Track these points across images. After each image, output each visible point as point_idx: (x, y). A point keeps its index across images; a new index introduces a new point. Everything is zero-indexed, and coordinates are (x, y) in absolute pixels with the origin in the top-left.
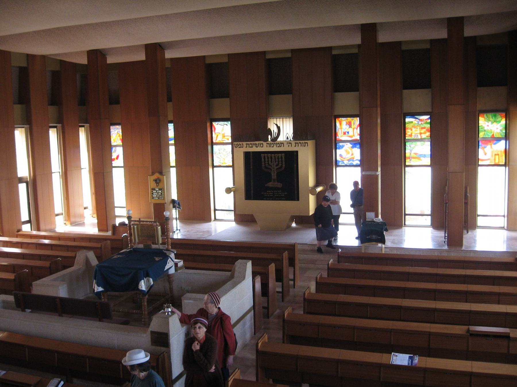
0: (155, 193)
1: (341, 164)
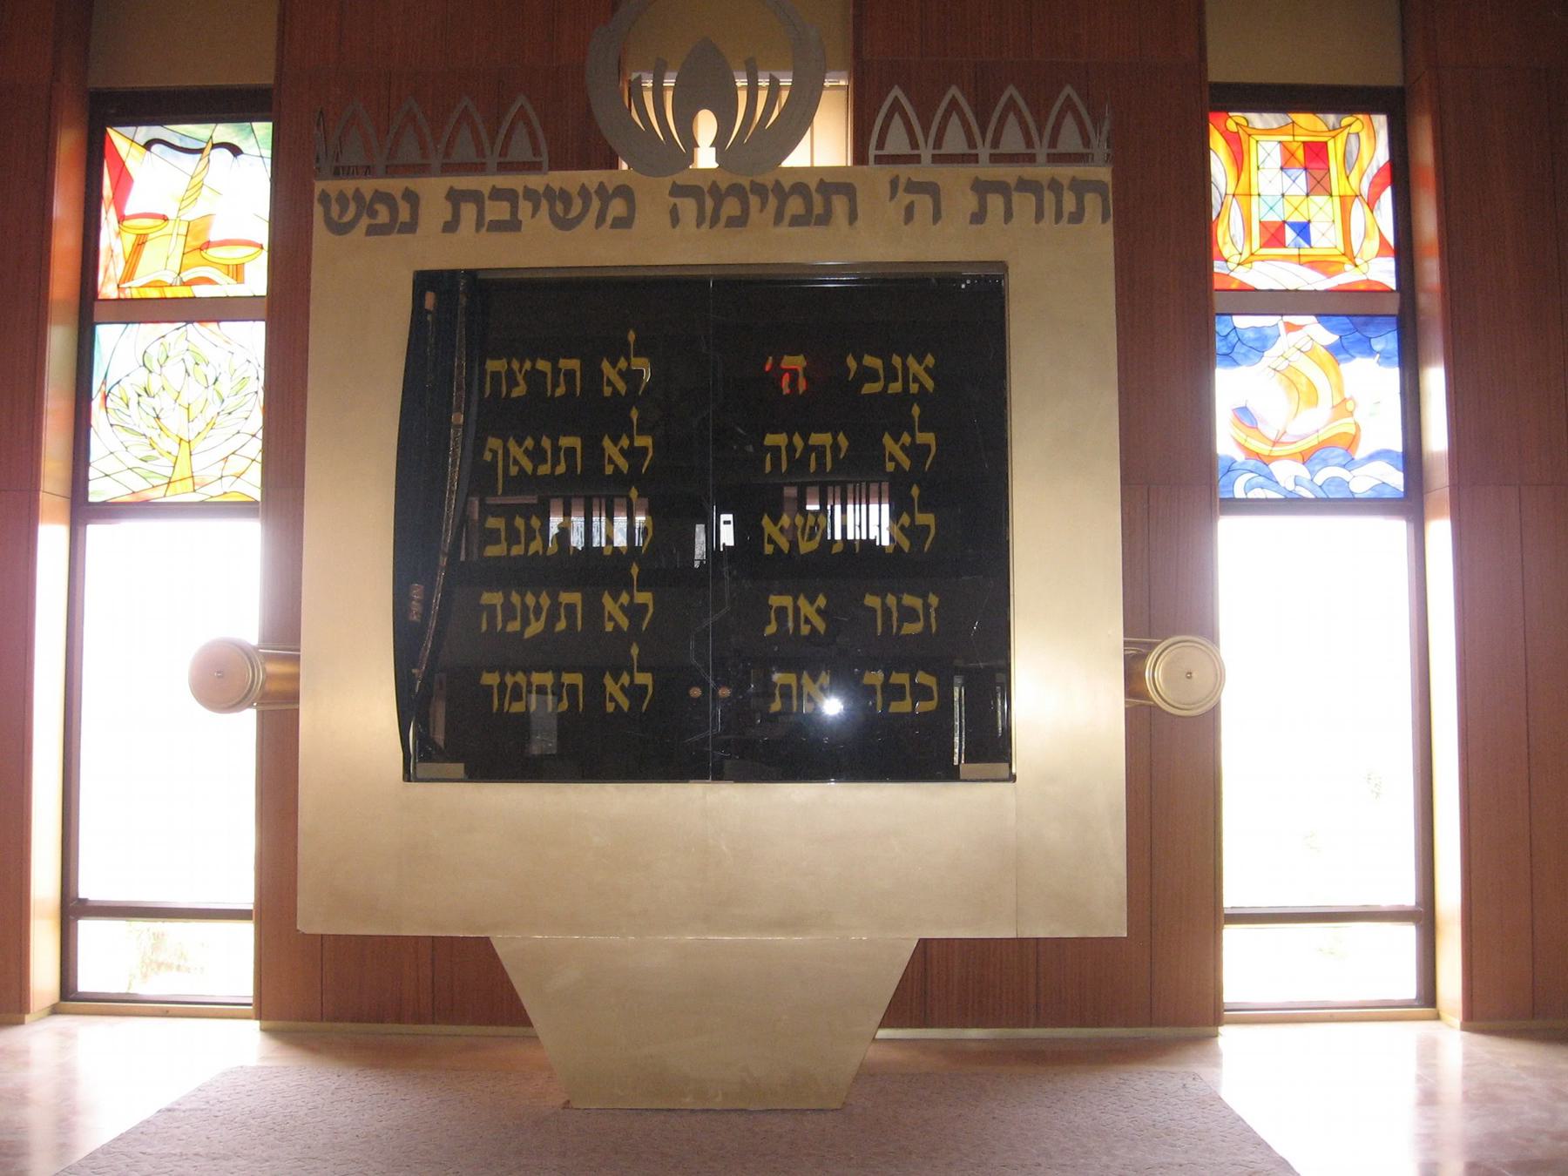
1: (1249, 487)
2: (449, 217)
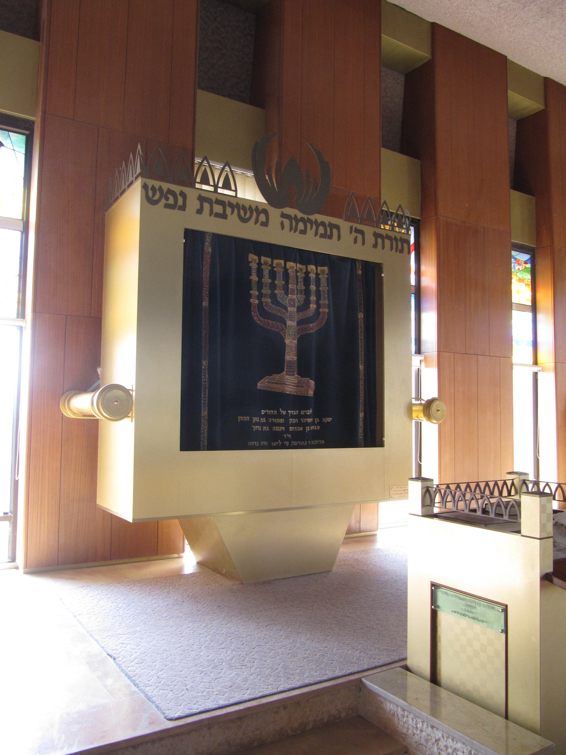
2: (199, 208)
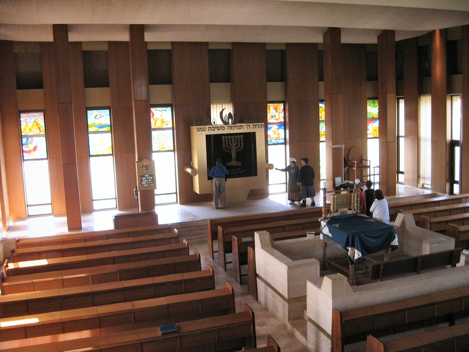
0: (145, 180)
2: (208, 129)
